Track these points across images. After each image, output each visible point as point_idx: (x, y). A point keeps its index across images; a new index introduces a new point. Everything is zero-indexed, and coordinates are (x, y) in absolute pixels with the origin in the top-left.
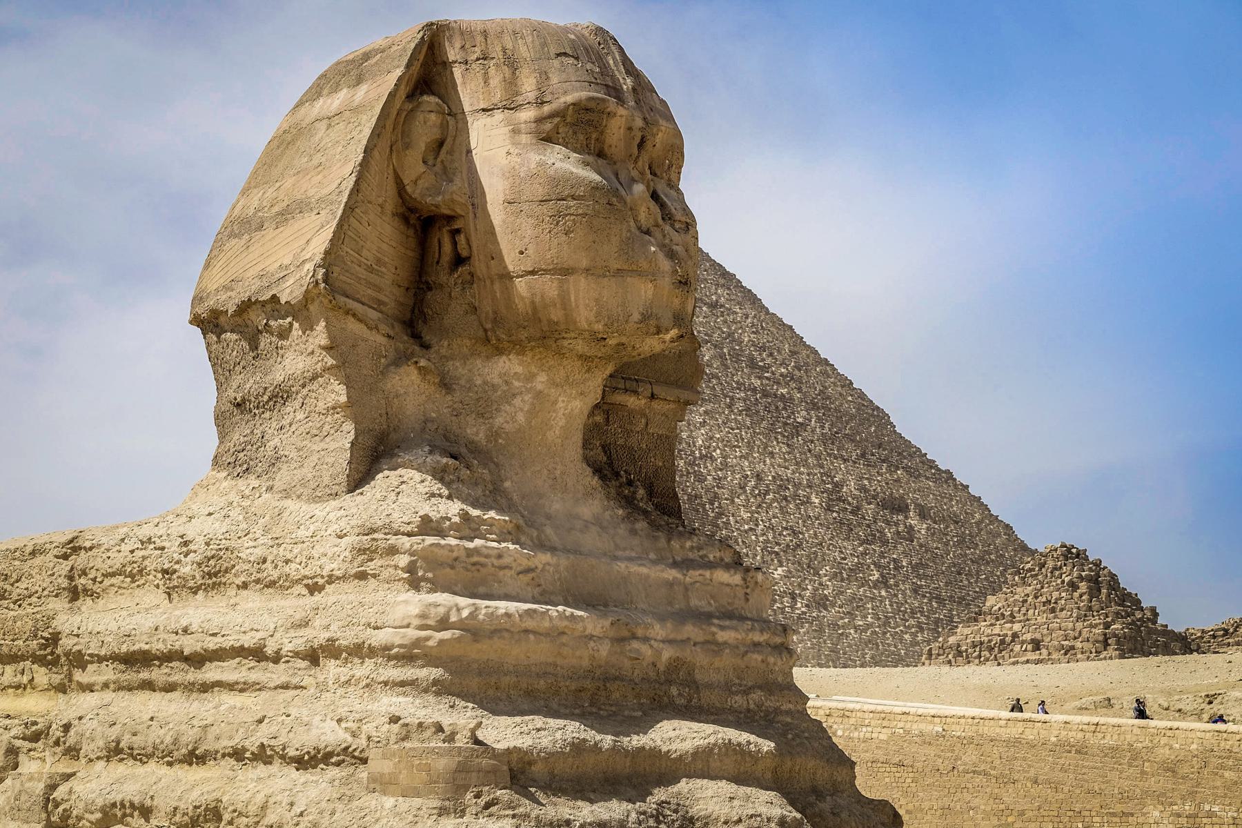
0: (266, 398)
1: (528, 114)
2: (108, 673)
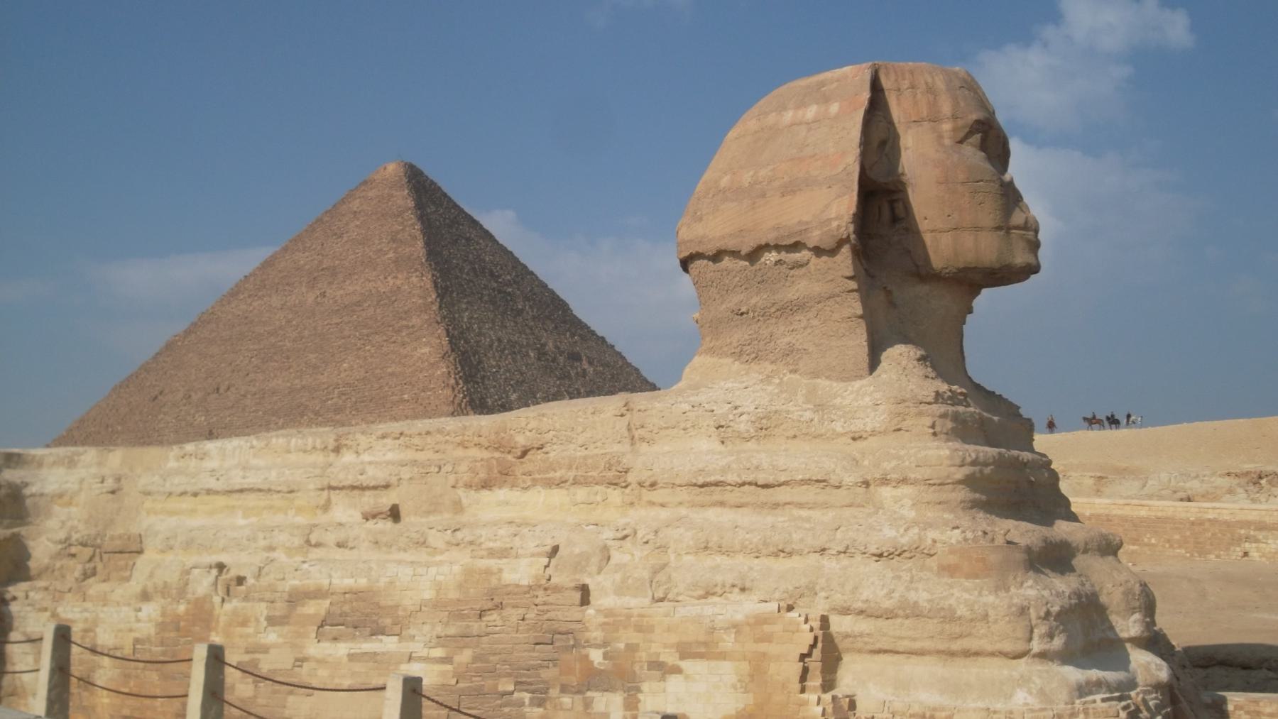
0: (773, 310)
1: (947, 127)
2: (683, 495)
